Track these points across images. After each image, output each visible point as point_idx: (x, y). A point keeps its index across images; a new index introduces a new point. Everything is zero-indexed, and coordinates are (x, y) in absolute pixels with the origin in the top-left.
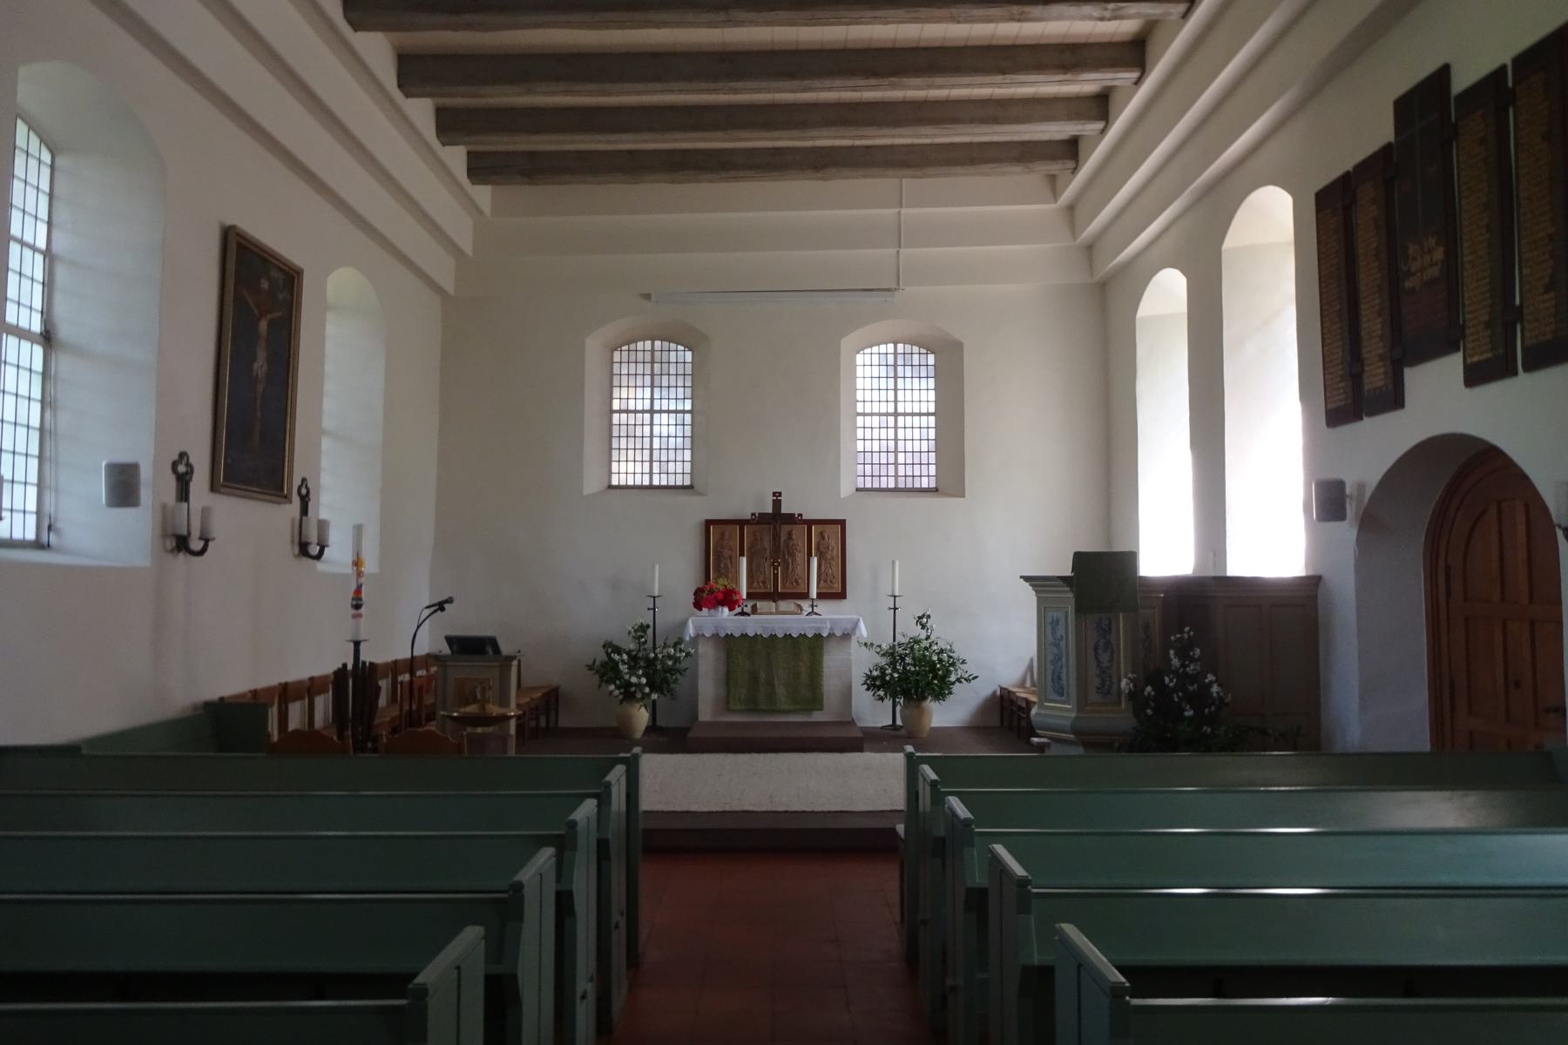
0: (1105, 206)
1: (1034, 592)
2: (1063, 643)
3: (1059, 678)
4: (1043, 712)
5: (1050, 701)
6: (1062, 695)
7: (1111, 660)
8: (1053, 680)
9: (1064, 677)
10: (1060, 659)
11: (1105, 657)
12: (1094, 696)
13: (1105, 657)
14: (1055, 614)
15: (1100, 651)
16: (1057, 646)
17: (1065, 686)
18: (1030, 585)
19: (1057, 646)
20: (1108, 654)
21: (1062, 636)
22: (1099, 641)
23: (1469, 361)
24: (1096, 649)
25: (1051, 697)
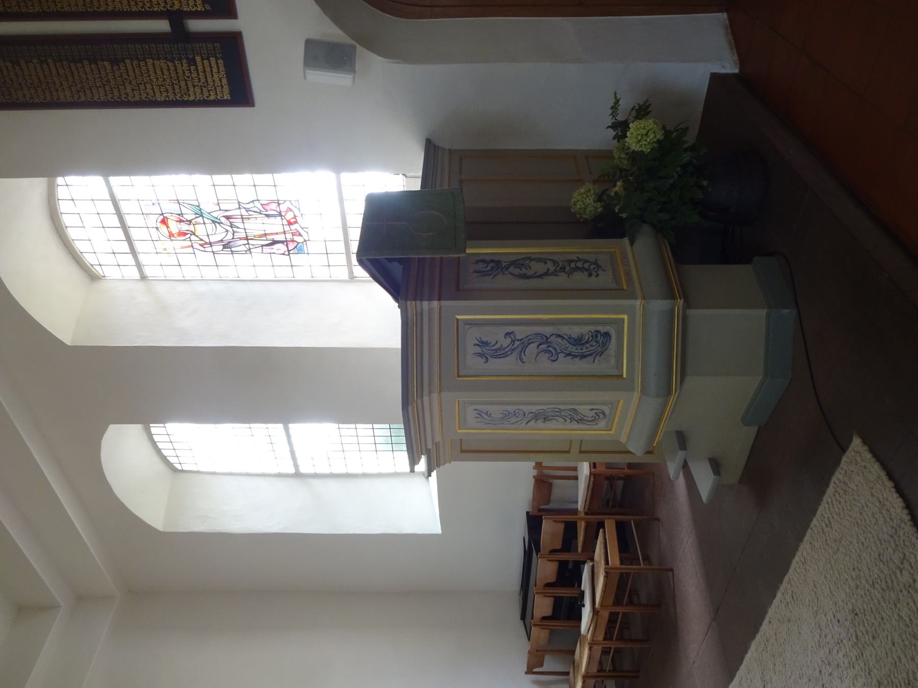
0: (75, 527)
1: (447, 465)
2: (521, 332)
3: (578, 341)
4: (638, 380)
5: (619, 365)
6: (607, 335)
7: (539, 260)
8: (583, 356)
9: (576, 331)
10: (545, 339)
11: (540, 268)
12: (604, 279)
13: (540, 268)
14: (472, 349)
15: (529, 273)
16: (525, 344)
17: (593, 328)
18: (444, 464)
19: (525, 344)
20: (533, 264)
21: (508, 334)
22: (512, 274)
23: (227, 97)
24: (525, 277)
25: (613, 361)
